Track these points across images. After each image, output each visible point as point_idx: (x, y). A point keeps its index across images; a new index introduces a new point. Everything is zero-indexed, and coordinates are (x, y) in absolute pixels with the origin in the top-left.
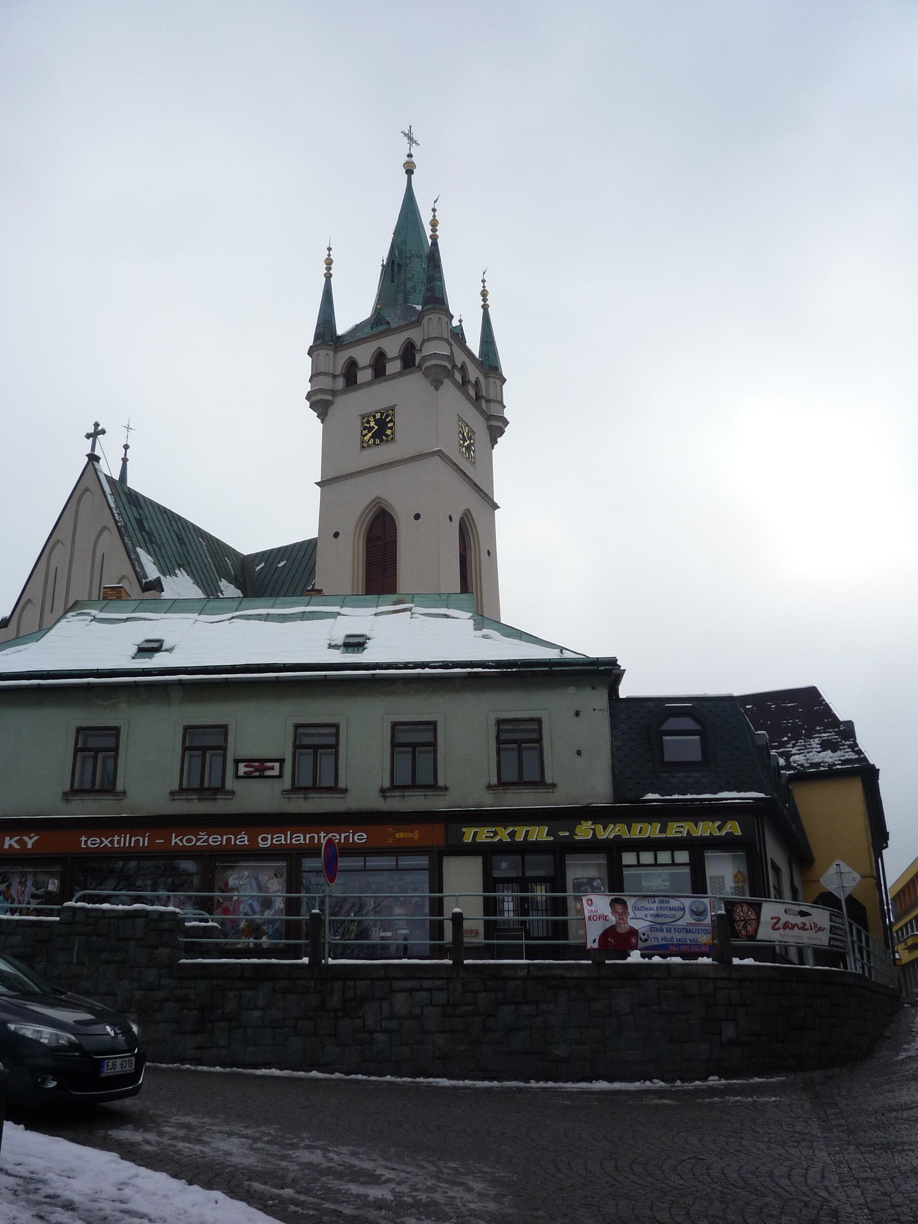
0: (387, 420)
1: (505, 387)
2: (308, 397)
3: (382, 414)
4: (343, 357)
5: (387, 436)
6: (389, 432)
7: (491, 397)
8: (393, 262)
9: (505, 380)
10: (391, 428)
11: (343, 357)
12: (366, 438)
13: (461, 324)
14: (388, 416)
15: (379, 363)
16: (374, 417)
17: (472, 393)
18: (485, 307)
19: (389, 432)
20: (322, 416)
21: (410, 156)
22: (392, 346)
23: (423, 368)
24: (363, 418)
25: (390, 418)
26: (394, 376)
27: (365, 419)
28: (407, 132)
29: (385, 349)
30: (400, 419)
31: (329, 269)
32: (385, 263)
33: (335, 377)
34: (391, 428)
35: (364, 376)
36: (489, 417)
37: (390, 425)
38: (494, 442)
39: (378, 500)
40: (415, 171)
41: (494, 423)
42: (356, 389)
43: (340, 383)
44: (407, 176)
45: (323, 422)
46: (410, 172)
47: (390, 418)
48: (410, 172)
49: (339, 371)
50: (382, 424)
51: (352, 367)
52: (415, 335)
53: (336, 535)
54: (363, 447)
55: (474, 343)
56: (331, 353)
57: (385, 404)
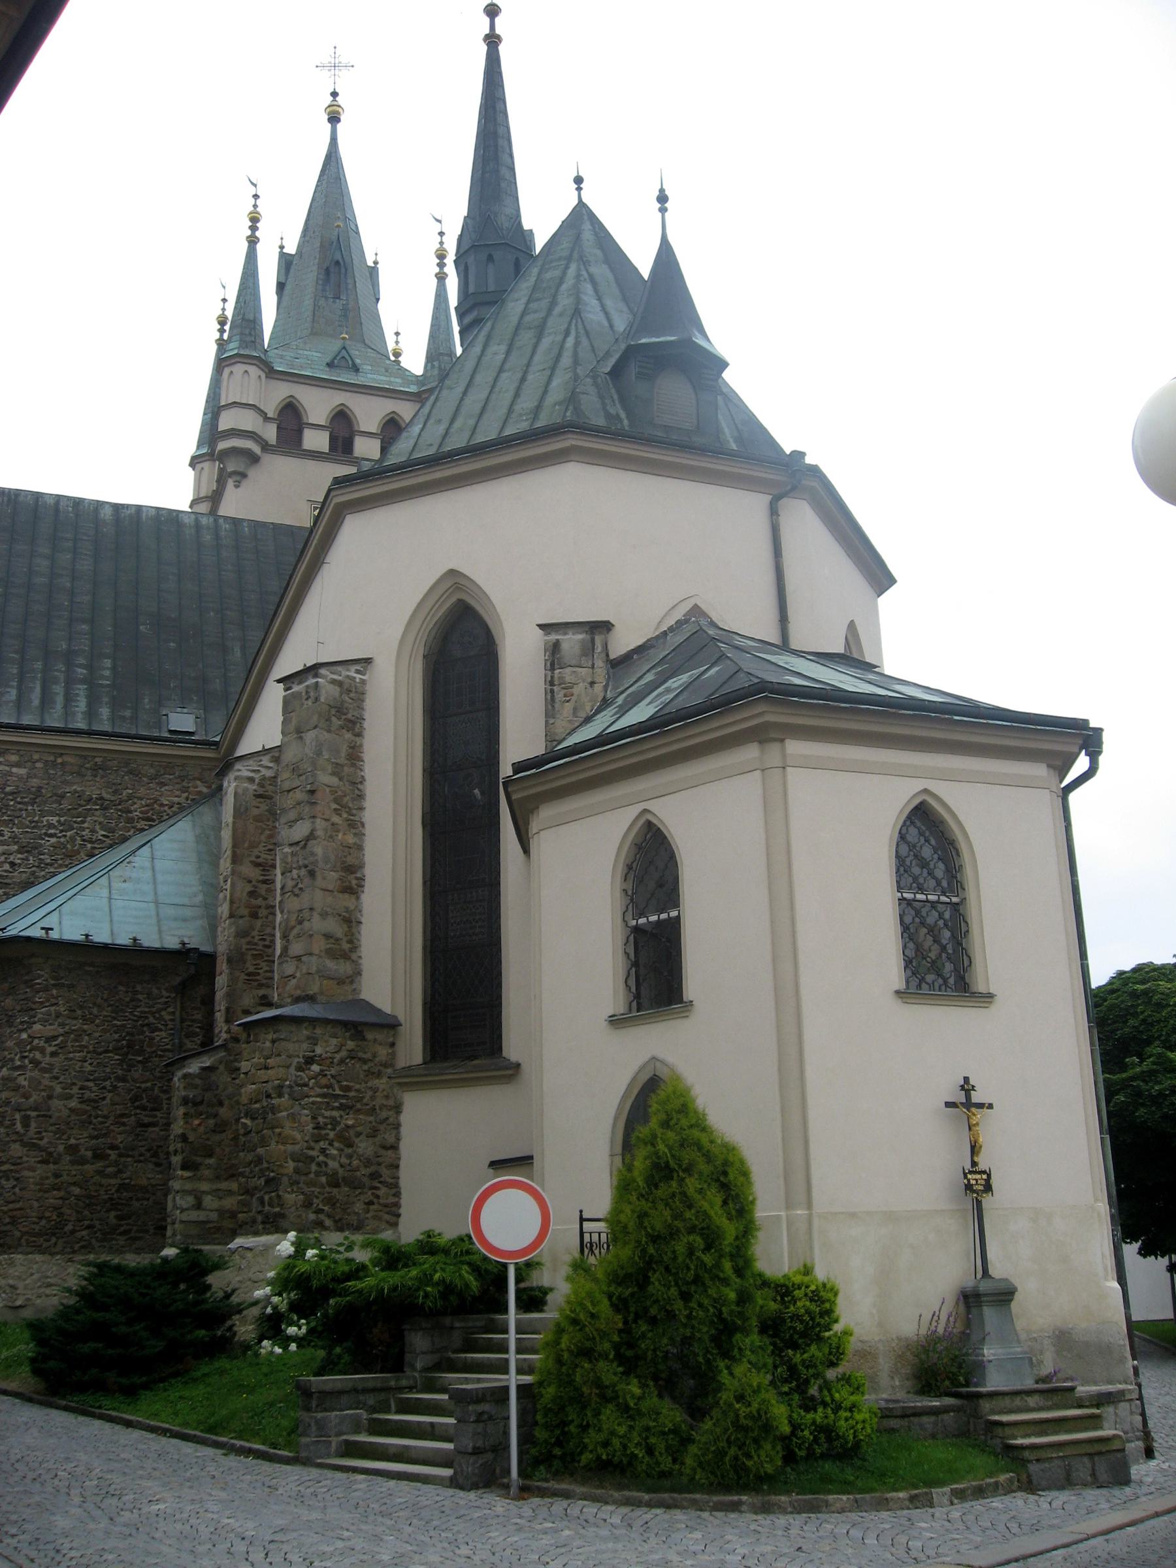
4: (281, 392)
11: (281, 392)
21: (334, 94)
31: (254, 228)
33: (266, 418)
40: (342, 118)
43: (270, 433)
44: (330, 125)
46: (334, 119)
48: (334, 119)
56: (263, 376)
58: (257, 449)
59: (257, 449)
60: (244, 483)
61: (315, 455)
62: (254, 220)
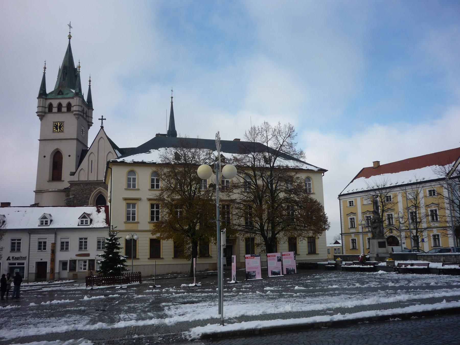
1: (93, 111)
2: (37, 113)
4: (48, 102)
5: (61, 130)
6: (62, 129)
9: (93, 110)
10: (62, 128)
11: (48, 102)
14: (62, 124)
15: (60, 106)
18: (90, 86)
19: (62, 129)
20: (41, 119)
22: (64, 103)
27: (54, 123)
28: (69, 24)
30: (65, 125)
32: (60, 68)
34: (62, 128)
35: (55, 110)
36: (88, 122)
37: (62, 127)
38: (89, 128)
39: (57, 149)
42: (52, 113)
43: (47, 110)
45: (41, 121)
46: (70, 39)
48: (70, 39)
49: (47, 106)
52: (71, 101)
55: (86, 98)
56: (44, 100)
60: (43, 120)
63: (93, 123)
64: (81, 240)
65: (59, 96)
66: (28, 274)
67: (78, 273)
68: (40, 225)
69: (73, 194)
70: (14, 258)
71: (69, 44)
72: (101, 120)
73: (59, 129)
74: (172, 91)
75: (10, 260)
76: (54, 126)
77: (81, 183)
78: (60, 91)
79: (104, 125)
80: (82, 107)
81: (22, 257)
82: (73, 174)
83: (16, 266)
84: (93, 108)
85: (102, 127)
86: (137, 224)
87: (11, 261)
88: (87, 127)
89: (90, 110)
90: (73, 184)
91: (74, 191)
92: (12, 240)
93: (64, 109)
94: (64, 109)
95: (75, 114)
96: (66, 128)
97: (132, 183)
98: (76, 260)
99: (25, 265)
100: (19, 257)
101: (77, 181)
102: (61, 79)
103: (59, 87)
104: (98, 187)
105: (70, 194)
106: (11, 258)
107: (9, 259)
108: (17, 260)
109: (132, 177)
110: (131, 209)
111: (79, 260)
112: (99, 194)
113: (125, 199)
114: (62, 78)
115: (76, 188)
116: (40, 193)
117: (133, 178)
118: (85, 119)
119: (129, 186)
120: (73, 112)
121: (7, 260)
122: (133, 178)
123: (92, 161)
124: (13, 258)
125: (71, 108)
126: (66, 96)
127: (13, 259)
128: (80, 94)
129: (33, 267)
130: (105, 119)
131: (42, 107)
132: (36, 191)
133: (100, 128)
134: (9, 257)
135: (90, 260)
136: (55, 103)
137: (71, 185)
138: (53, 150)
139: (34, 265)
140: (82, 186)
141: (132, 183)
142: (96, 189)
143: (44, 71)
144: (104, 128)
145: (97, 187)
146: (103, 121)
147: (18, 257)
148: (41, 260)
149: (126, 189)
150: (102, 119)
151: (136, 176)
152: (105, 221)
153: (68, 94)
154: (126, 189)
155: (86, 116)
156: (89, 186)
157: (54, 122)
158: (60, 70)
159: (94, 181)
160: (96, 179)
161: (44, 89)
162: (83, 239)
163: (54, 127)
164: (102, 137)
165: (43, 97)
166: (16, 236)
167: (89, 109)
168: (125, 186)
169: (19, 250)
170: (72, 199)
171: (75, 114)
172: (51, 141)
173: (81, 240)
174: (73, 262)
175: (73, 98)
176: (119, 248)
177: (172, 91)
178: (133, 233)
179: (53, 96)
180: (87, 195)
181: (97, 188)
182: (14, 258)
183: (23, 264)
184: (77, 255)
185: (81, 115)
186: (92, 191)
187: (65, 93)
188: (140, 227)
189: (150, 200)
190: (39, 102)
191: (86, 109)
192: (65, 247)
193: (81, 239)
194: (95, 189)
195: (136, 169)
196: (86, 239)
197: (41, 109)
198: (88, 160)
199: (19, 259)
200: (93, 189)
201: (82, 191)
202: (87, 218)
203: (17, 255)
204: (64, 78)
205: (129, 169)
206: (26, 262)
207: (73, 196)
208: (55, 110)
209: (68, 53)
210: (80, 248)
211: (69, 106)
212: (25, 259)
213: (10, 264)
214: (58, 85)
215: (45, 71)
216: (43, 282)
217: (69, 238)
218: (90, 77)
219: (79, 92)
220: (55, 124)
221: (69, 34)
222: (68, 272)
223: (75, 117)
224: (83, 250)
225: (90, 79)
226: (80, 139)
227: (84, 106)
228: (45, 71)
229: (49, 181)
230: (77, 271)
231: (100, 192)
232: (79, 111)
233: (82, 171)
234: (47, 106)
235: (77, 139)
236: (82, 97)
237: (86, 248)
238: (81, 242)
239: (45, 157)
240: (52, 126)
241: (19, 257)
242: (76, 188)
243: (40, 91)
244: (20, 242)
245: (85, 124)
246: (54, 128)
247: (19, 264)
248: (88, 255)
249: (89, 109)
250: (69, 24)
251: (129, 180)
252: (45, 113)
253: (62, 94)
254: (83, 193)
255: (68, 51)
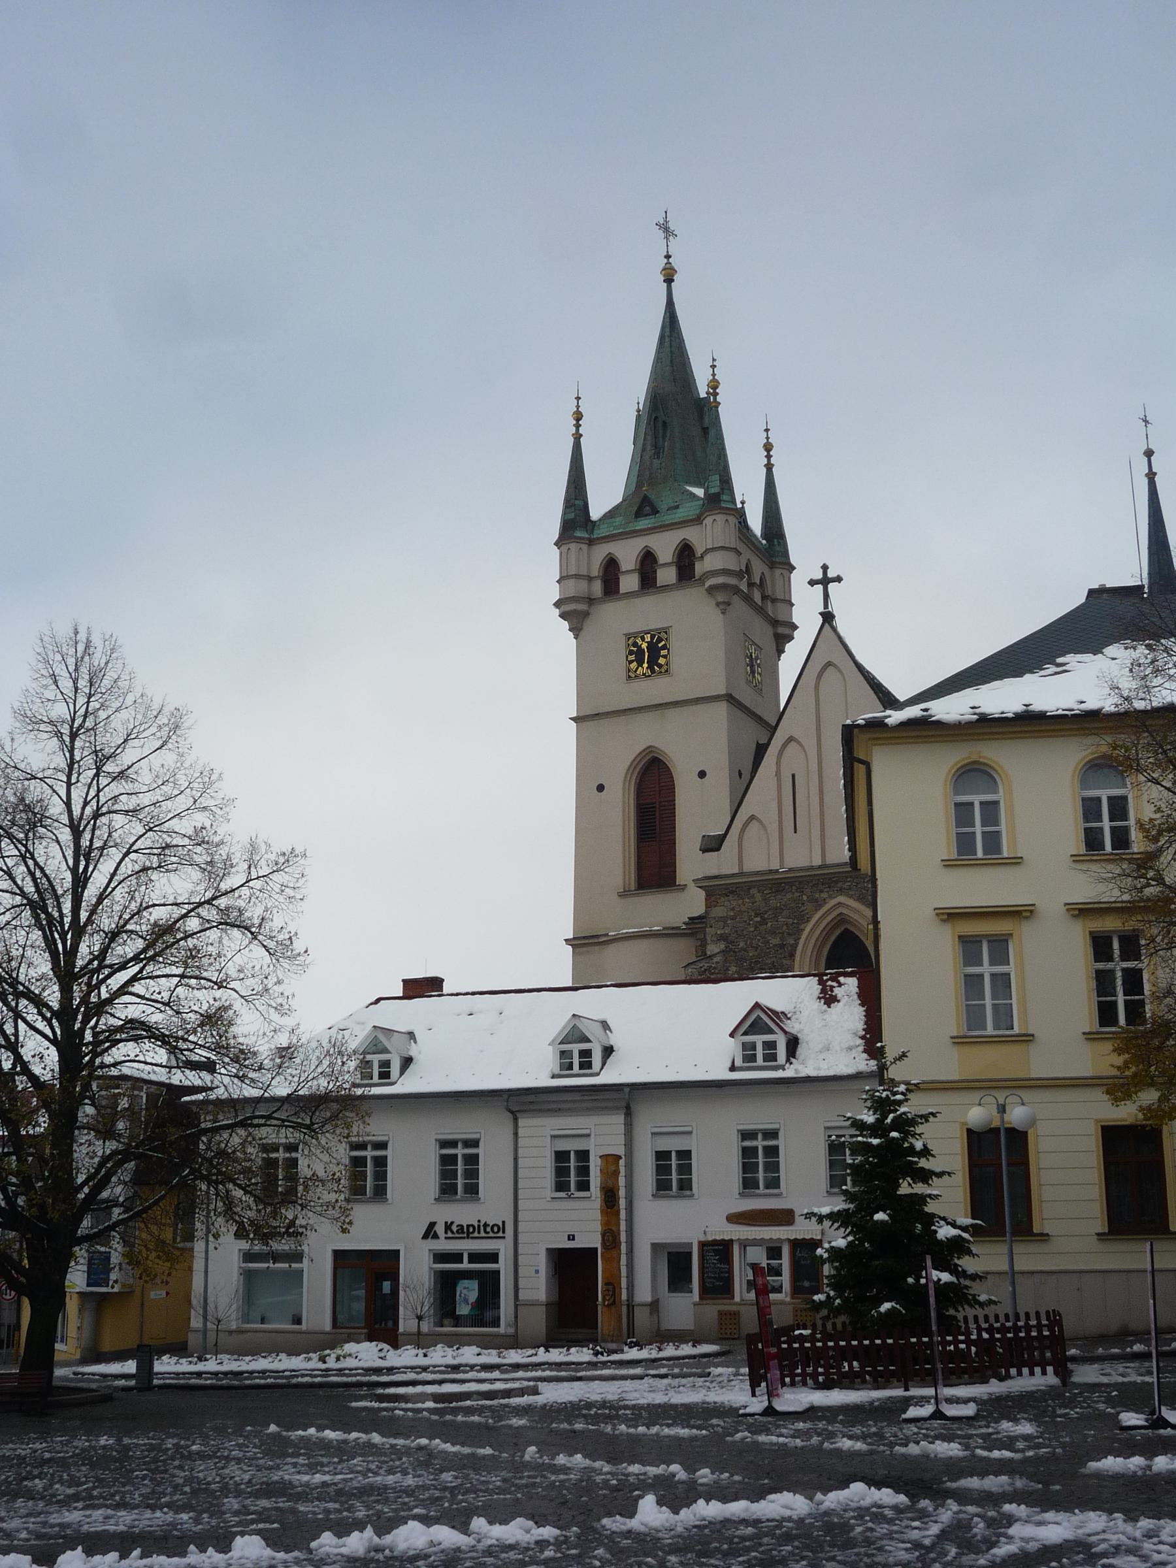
0: (660, 645)
2: (557, 604)
3: (652, 637)
4: (600, 553)
5: (660, 666)
6: (662, 661)
7: (780, 596)
8: (656, 418)
9: (794, 568)
10: (665, 657)
11: (600, 553)
12: (634, 665)
13: (743, 507)
14: (659, 640)
15: (648, 562)
16: (643, 638)
17: (757, 597)
19: (662, 661)
20: (576, 630)
21: (668, 257)
22: (665, 546)
23: (707, 584)
24: (629, 639)
25: (663, 643)
26: (666, 588)
28: (662, 222)
29: (655, 548)
30: (675, 644)
32: (641, 408)
34: (665, 657)
35: (628, 583)
36: (775, 623)
37: (663, 652)
38: (780, 651)
39: (650, 749)
41: (781, 630)
42: (620, 599)
43: (597, 588)
46: (669, 280)
47: (663, 643)
48: (669, 280)
49: (595, 572)
50: (654, 650)
51: (611, 567)
52: (691, 534)
53: (601, 788)
54: (629, 677)
55: (755, 522)
56: (585, 547)
57: (654, 625)
58: (582, 607)
59: (582, 607)
60: (582, 634)
61: (630, 595)
62: (578, 416)
63: (795, 627)
64: (747, 1143)
65: (644, 523)
66: (516, 1306)
67: (743, 1309)
68: (557, 1071)
69: (722, 938)
70: (454, 1228)
71: (670, 304)
72: (820, 587)
73: (645, 665)
74: (1146, 422)
75: (436, 1236)
76: (631, 652)
77: (750, 886)
78: (646, 500)
79: (836, 607)
80: (739, 553)
81: (486, 1225)
82: (712, 845)
83: (465, 1265)
84: (793, 561)
85: (828, 617)
86: (1025, 1044)
87: (444, 1245)
88: (769, 645)
89: (778, 572)
90: (715, 889)
91: (724, 919)
92: (444, 1144)
93: (667, 575)
94: (667, 575)
95: (711, 590)
96: (679, 655)
97: (978, 829)
98: (731, 1241)
99: (504, 1266)
100: (476, 1224)
101: (733, 875)
102: (644, 450)
103: (639, 486)
104: (831, 897)
105: (708, 938)
106: (440, 1229)
107: (430, 1233)
108: (468, 1237)
109: (976, 799)
110: (986, 969)
111: (745, 1244)
112: (838, 932)
113: (950, 916)
114: (649, 447)
115: (733, 909)
116: (590, 949)
117: (982, 803)
118: (760, 611)
119: (965, 843)
120: (702, 580)
121: (425, 1237)
122: (982, 803)
123: (793, 776)
124: (448, 1227)
125: (692, 566)
126: (668, 519)
127: (450, 1235)
128: (725, 497)
129: (537, 1272)
130: (839, 579)
131: (577, 576)
132: (574, 938)
133: (820, 620)
134: (432, 1225)
135: (796, 1244)
136: (627, 554)
137: (709, 896)
138: (633, 757)
139: (542, 1262)
140: (758, 897)
141: (978, 829)
142: (820, 906)
143: (574, 430)
144: (840, 623)
145: (824, 895)
146: (831, 586)
147: (468, 1226)
148: (571, 1238)
149: (948, 864)
150: (825, 581)
151: (996, 791)
152: (860, 1041)
153: (677, 507)
154: (948, 864)
155: (764, 597)
156: (789, 896)
157: (628, 636)
158: (638, 417)
159: (812, 868)
160: (817, 861)
161: (577, 502)
162: (760, 1136)
163: (632, 657)
164: (829, 664)
165: (578, 534)
166: (458, 1126)
167: (772, 566)
168: (942, 844)
169: (472, 1190)
170: (715, 960)
171: (711, 590)
172: (622, 719)
173: (747, 1143)
174: (719, 1251)
175: (698, 520)
176: (925, 1176)
177: (1146, 422)
178: (1001, 1096)
179: (615, 528)
180: (782, 939)
181: (825, 901)
182: (454, 1228)
183: (493, 1257)
184: (736, 1218)
185: (736, 590)
186: (803, 919)
187: (663, 506)
188: (1041, 1064)
189: (1082, 911)
190: (564, 561)
191: (758, 568)
192: (674, 1176)
193: (746, 1135)
194: (818, 904)
195: (995, 753)
196: (772, 1134)
197: (573, 588)
198: (778, 773)
199: (476, 1234)
200: (809, 907)
201: (758, 919)
202: (771, 1032)
203: (463, 1213)
204: (655, 446)
205: (952, 756)
206: (503, 1247)
207: (722, 946)
208: (628, 583)
209: (667, 339)
210: (749, 1184)
211: (686, 557)
212: (500, 1234)
213: (440, 1257)
214: (635, 480)
215: (578, 426)
216: (573, 1350)
217: (690, 1133)
218: (767, 430)
219: (722, 489)
220: (635, 644)
221: (666, 261)
222: (695, 1304)
223: (714, 603)
224: (762, 1189)
225: (768, 438)
226: (745, 695)
227: (747, 554)
228: (578, 426)
229: (624, 894)
230: (737, 1299)
231: (842, 919)
232: (725, 572)
233: (754, 826)
234: (596, 570)
235: (730, 698)
236: (740, 515)
237: (774, 1183)
238: (748, 1153)
239: (601, 788)
240: (623, 653)
241: (476, 1224)
242: (733, 909)
243: (564, 513)
244: (477, 1155)
245: (762, 633)
246: (631, 662)
247: (475, 1257)
248: (785, 1217)
249: (772, 566)
250: (662, 222)
251: (963, 812)
252: (591, 601)
253: (655, 512)
254: (763, 928)
255: (667, 334)
